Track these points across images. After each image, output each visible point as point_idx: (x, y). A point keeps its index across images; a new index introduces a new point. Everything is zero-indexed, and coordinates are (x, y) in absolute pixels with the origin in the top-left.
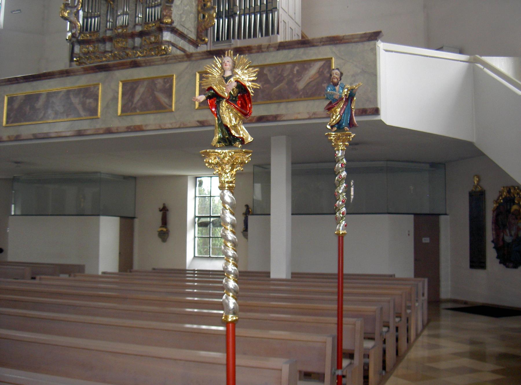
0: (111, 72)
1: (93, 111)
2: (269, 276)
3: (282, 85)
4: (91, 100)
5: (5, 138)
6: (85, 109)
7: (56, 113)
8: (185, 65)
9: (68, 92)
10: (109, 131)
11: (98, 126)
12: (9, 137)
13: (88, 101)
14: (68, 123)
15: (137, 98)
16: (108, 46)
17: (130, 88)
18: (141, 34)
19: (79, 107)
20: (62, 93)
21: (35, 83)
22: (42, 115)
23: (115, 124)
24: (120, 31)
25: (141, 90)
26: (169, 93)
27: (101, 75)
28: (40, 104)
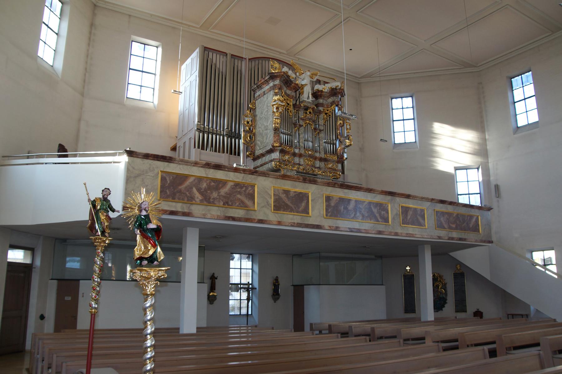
0: (395, 197)
1: (386, 220)
2: (420, 320)
3: (465, 224)
4: (384, 212)
5: (327, 228)
6: (381, 217)
7: (363, 216)
8: (429, 203)
9: (370, 203)
10: (396, 234)
11: (390, 230)
12: (330, 226)
13: (383, 213)
14: (372, 225)
15: (409, 217)
16: (297, 160)
17: (405, 210)
18: (321, 160)
19: (377, 215)
20: (366, 203)
21: (346, 191)
22: (353, 215)
23: (399, 231)
24: (310, 153)
25: (410, 213)
26: (423, 217)
27: (389, 198)
28: (351, 206)
